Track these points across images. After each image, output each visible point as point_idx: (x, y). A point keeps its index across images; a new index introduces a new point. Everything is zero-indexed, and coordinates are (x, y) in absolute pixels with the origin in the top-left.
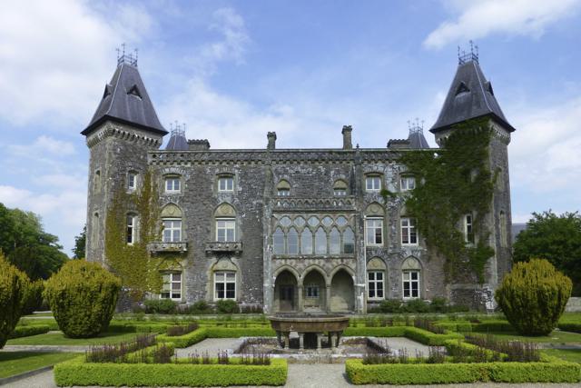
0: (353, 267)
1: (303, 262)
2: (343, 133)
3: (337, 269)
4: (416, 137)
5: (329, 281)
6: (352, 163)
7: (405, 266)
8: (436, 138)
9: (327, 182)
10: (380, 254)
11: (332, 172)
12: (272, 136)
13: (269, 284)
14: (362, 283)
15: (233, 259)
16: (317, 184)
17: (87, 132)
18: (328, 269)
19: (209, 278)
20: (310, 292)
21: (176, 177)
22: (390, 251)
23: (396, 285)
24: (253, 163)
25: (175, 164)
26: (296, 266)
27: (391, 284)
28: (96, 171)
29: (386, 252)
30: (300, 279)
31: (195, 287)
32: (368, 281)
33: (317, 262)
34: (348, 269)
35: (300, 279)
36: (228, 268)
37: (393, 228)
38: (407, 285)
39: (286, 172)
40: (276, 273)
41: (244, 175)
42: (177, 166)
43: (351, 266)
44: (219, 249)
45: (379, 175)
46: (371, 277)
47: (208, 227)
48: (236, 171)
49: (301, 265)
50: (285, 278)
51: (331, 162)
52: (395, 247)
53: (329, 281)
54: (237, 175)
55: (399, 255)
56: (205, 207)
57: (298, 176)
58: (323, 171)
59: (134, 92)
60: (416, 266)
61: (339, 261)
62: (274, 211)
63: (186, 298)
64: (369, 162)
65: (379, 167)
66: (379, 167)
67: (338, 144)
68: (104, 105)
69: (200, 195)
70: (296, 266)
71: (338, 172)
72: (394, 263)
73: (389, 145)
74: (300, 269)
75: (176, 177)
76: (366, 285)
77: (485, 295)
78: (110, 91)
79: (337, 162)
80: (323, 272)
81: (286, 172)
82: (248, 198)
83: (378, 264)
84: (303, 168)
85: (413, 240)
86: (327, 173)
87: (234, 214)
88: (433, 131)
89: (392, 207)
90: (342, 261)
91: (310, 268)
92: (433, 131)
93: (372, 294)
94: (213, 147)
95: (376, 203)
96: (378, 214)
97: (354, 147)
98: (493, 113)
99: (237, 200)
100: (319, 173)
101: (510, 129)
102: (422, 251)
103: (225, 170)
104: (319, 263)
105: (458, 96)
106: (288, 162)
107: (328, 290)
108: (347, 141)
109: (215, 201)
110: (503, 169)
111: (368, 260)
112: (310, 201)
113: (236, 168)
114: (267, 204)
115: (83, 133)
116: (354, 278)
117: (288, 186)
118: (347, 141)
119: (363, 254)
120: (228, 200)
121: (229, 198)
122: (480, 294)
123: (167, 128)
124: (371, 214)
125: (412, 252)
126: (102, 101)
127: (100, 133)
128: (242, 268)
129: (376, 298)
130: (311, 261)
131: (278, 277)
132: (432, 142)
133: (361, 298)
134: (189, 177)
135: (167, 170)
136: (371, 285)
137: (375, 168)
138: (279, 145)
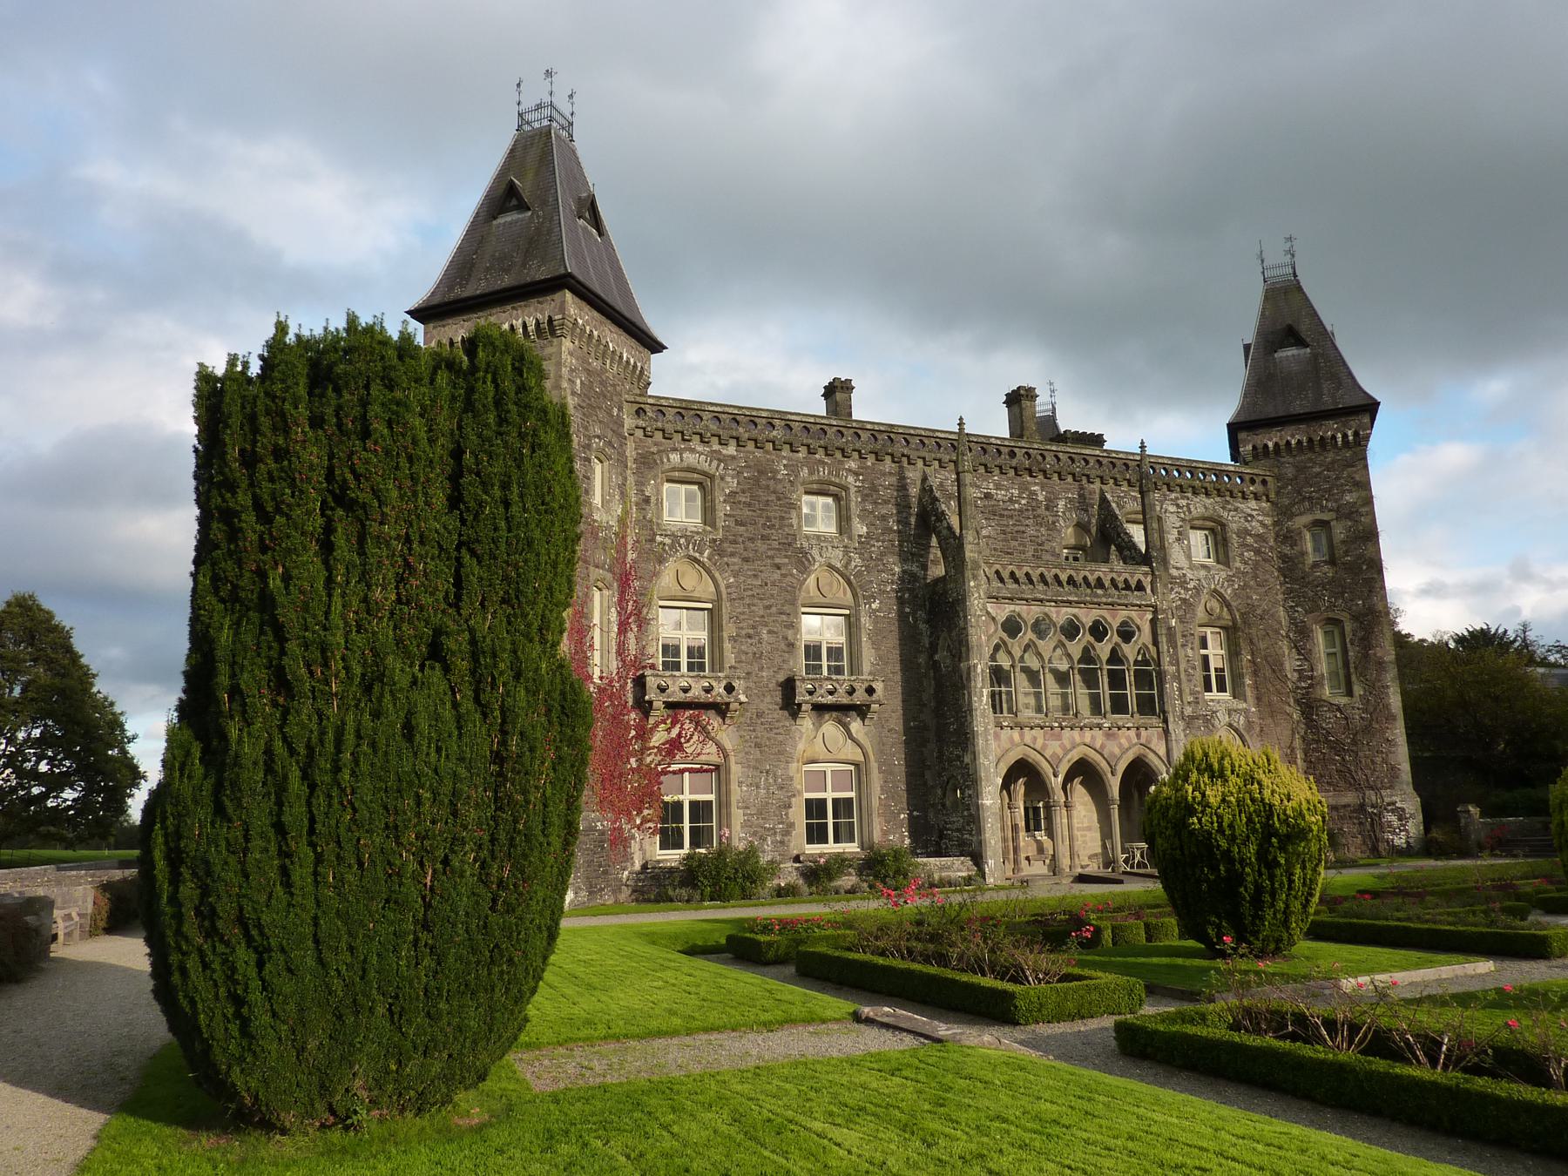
1: (1059, 738)
11: (1061, 503)
16: (1031, 531)
25: (695, 443)
34: (1151, 756)
42: (700, 448)
47: (790, 633)
48: (851, 479)
54: (853, 490)
56: (777, 575)
58: (1041, 498)
69: (764, 538)
70: (1044, 746)
77: (1393, 818)
80: (1104, 764)
82: (882, 554)
84: (998, 487)
85: (1221, 688)
89: (1184, 601)
91: (1075, 756)
99: (857, 560)
102: (1246, 711)
103: (823, 473)
104: (1093, 737)
113: (850, 470)
122: (1380, 815)
134: (732, 483)
135: (675, 457)
138: (863, 410)
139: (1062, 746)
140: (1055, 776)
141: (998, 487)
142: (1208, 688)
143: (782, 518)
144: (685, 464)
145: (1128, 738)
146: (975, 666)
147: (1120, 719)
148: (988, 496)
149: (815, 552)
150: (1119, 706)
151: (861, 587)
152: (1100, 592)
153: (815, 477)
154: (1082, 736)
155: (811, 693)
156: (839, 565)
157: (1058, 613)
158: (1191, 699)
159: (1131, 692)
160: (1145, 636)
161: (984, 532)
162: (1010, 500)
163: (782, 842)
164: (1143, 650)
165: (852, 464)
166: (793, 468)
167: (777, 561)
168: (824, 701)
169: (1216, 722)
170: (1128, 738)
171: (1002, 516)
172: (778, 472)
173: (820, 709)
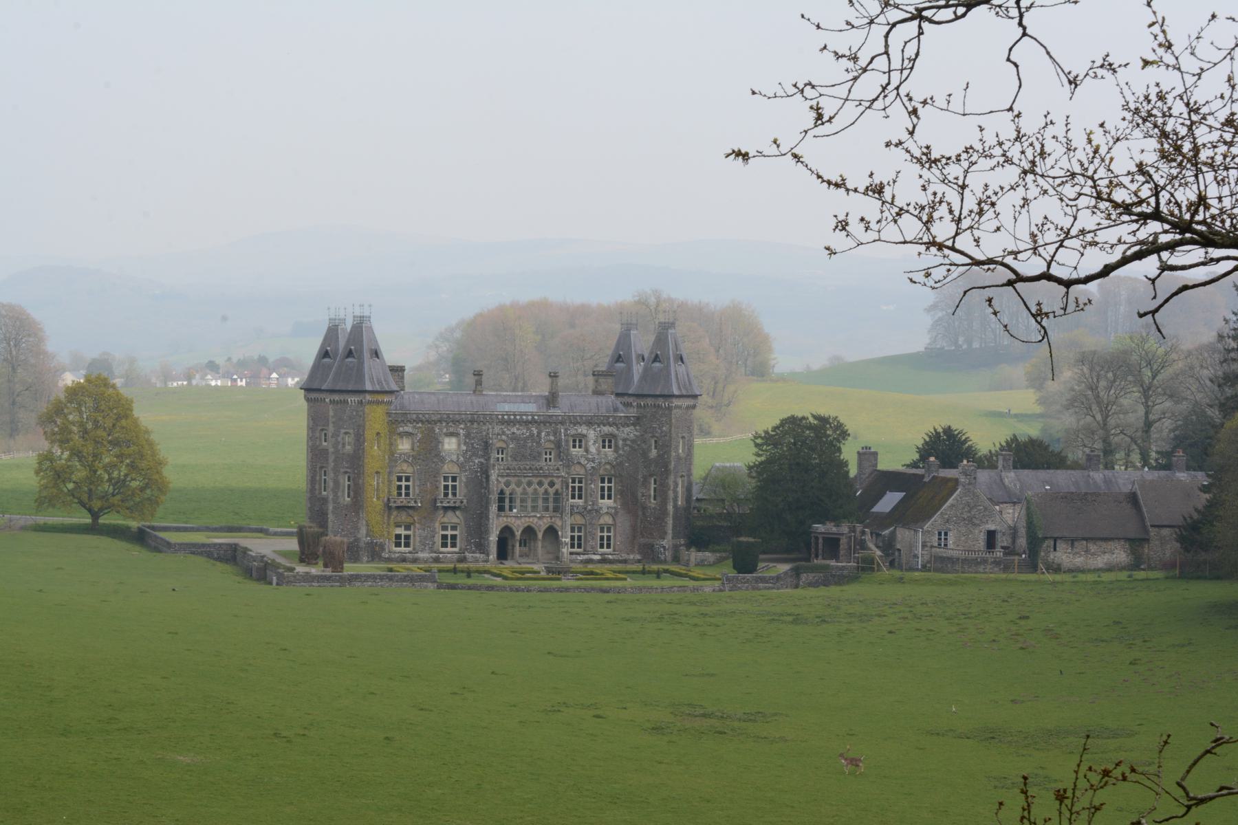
5: (540, 535)
7: (602, 521)
9: (538, 443)
13: (493, 538)
15: (458, 513)
20: (523, 543)
21: (408, 434)
27: (589, 538)
30: (518, 534)
32: (569, 534)
35: (518, 534)
38: (602, 538)
39: (504, 433)
41: (467, 436)
43: (559, 523)
46: (573, 530)
49: (518, 522)
50: (506, 532)
53: (540, 535)
55: (597, 511)
57: (514, 438)
65: (583, 430)
66: (583, 430)
71: (548, 434)
75: (408, 434)
76: (568, 540)
83: (579, 520)
85: (609, 498)
86: (539, 434)
93: (572, 546)
95: (579, 463)
100: (532, 435)
102: (615, 508)
103: (451, 430)
107: (540, 544)
109: (443, 460)
120: (454, 458)
129: (576, 550)
133: (565, 550)
136: (572, 538)
142: (603, 498)
150: (547, 509)
159: (551, 505)
173: (446, 509)
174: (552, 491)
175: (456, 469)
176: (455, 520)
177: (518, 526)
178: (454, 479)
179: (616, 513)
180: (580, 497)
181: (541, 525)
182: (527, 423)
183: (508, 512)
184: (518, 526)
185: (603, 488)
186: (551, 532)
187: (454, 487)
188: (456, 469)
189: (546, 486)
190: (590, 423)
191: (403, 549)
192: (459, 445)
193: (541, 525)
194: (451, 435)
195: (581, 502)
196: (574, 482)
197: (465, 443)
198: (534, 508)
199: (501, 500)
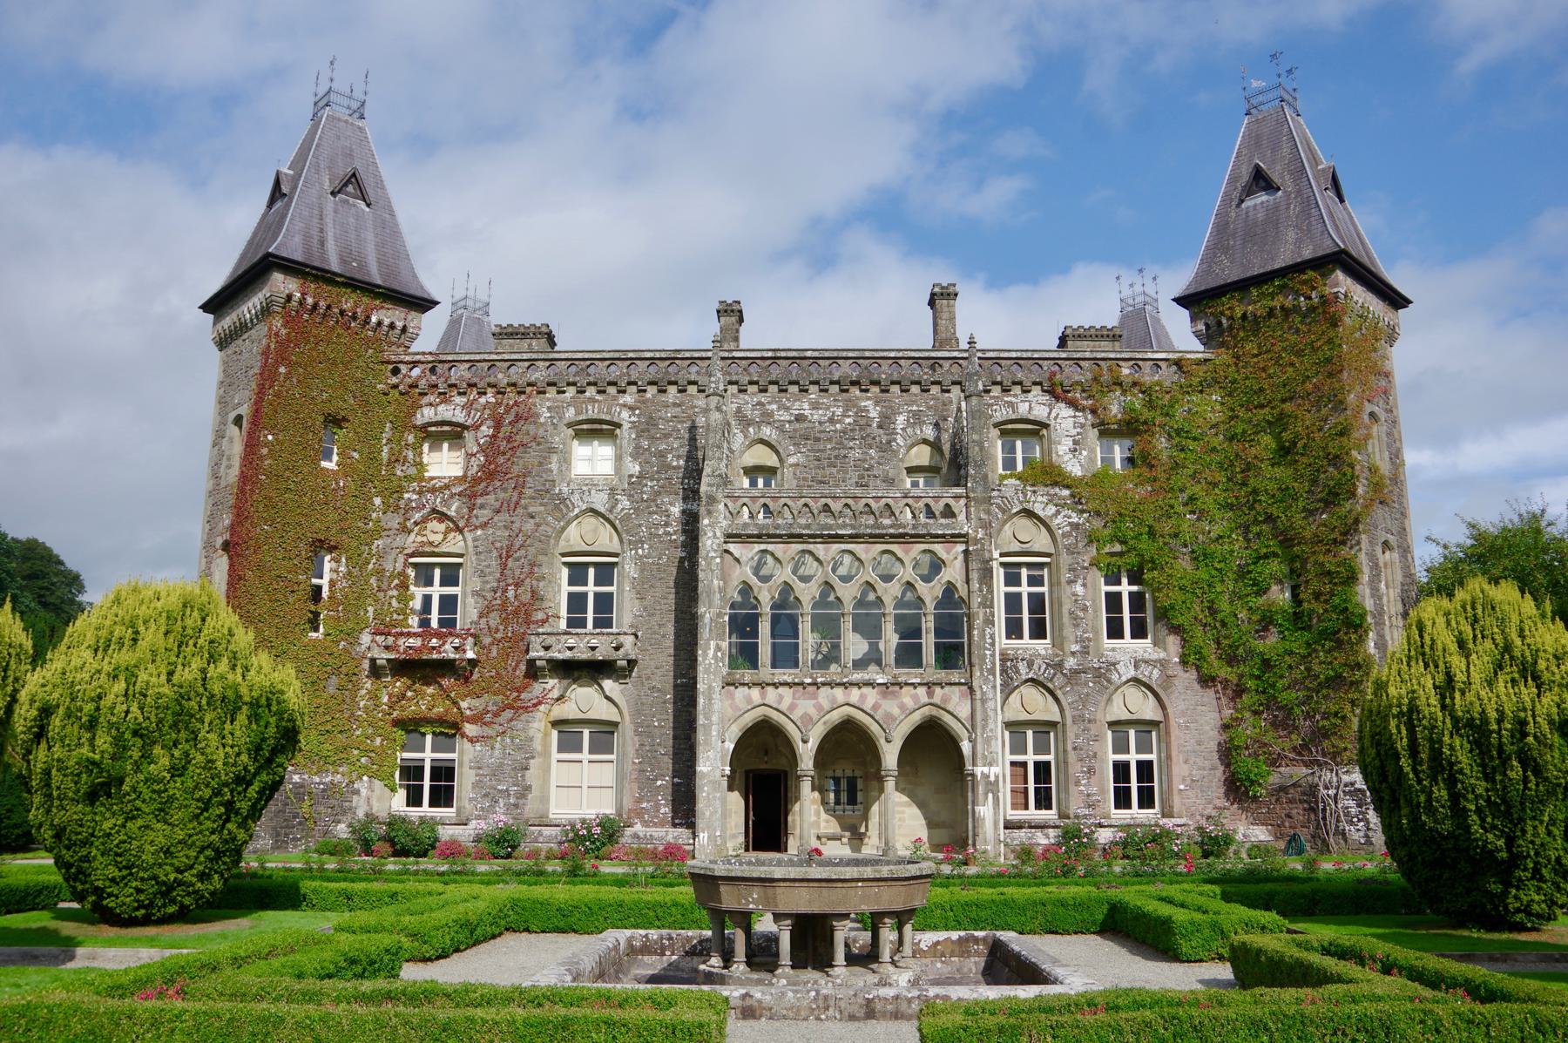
0: (964, 711)
1: (814, 697)
2: (932, 303)
3: (917, 718)
4: (1136, 326)
5: (890, 756)
6: (956, 390)
7: (1117, 712)
8: (1193, 319)
9: (886, 448)
10: (1040, 670)
11: (901, 419)
12: (731, 313)
13: (713, 762)
14: (993, 763)
16: (857, 454)
17: (217, 305)
18: (889, 717)
19: (537, 745)
21: (453, 434)
22: (1071, 663)
23: (1091, 771)
24: (672, 390)
26: (792, 707)
27: (1076, 768)
28: (232, 415)
29: (1059, 666)
30: (806, 754)
31: (496, 772)
33: (855, 695)
34: (947, 718)
35: (806, 754)
36: (592, 715)
37: (1079, 589)
38: (1121, 770)
39: (767, 418)
40: (735, 732)
41: (646, 428)
44: (568, 655)
45: (1036, 430)
48: (625, 414)
51: (895, 389)
52: (1085, 651)
53: (890, 756)
54: (626, 426)
57: (803, 434)
58: (873, 414)
59: (350, 188)
60: (1149, 710)
61: (922, 691)
62: (730, 537)
63: (468, 806)
64: (1006, 391)
65: (1035, 405)
66: (1035, 405)
67: (916, 334)
68: (269, 226)
70: (792, 707)
71: (916, 419)
72: (1084, 700)
73: (1063, 341)
74: (807, 719)
78: (285, 189)
79: (915, 389)
80: (874, 728)
81: (767, 418)
84: (815, 406)
85: (1139, 631)
86: (886, 422)
87: (615, 546)
88: (1181, 301)
90: (930, 694)
91: (836, 717)
92: (1181, 301)
94: (566, 342)
95: (1029, 514)
96: (1036, 548)
97: (964, 345)
98: (1344, 252)
99: (625, 503)
100: (862, 422)
101: (1396, 300)
102: (1163, 664)
103: (592, 412)
104: (863, 697)
105: (1249, 203)
106: (773, 389)
108: (943, 337)
110: (1382, 416)
111: (1008, 689)
112: (836, 506)
114: (709, 513)
115: (208, 307)
116: (966, 747)
117: (771, 460)
118: (943, 337)
119: (992, 671)
120: (600, 501)
121: (604, 496)
123: (433, 289)
124: (1016, 547)
125: (1136, 667)
126: (264, 216)
127: (249, 307)
128: (637, 713)
130: (839, 693)
131: (740, 745)
132: (1181, 333)
133: (985, 811)
137: (1023, 409)
139: (819, 707)
140: (805, 742)
141: (815, 406)
142: (1115, 631)
143: (541, 464)
144: (439, 418)
145: (915, 698)
146: (703, 616)
147: (911, 675)
148: (800, 418)
149: (575, 498)
151: (628, 532)
152: (887, 522)
153: (583, 417)
154: (763, 696)
155: (547, 648)
156: (602, 510)
157: (827, 550)
158: (1075, 647)
159: (928, 642)
160: (953, 572)
161: (792, 460)
162: (831, 421)
163: (516, 806)
164: (950, 588)
165: (628, 399)
166: (556, 410)
167: (531, 509)
168: (560, 656)
169: (1115, 677)
170: (915, 698)
171: (817, 440)
172: (538, 416)
174: (930, 593)
175: (606, 539)
176: (604, 711)
177: (807, 717)
178: (605, 573)
179: (1168, 679)
180: (1038, 631)
181: (893, 715)
182: (844, 385)
183: (766, 671)
184: (807, 717)
185: (1113, 601)
186: (934, 749)
187: (604, 602)
188: (606, 539)
189: (907, 573)
190: (1056, 392)
191: (426, 809)
192: (619, 458)
193: (893, 715)
194: (597, 430)
195: (1042, 646)
196: (1012, 580)
197: (635, 456)
198: (873, 658)
199: (743, 625)
